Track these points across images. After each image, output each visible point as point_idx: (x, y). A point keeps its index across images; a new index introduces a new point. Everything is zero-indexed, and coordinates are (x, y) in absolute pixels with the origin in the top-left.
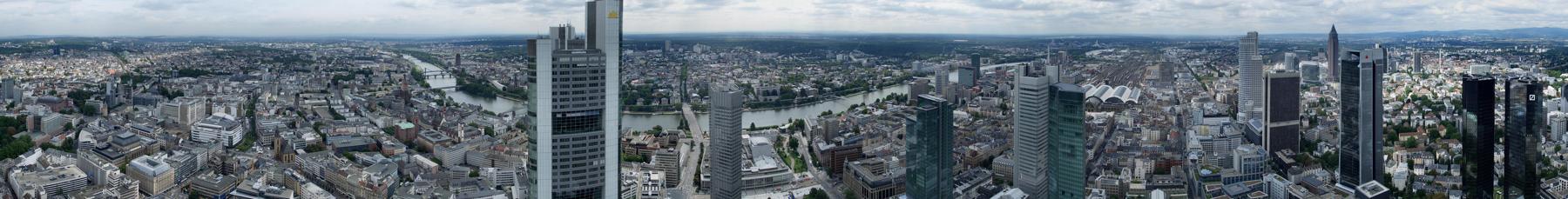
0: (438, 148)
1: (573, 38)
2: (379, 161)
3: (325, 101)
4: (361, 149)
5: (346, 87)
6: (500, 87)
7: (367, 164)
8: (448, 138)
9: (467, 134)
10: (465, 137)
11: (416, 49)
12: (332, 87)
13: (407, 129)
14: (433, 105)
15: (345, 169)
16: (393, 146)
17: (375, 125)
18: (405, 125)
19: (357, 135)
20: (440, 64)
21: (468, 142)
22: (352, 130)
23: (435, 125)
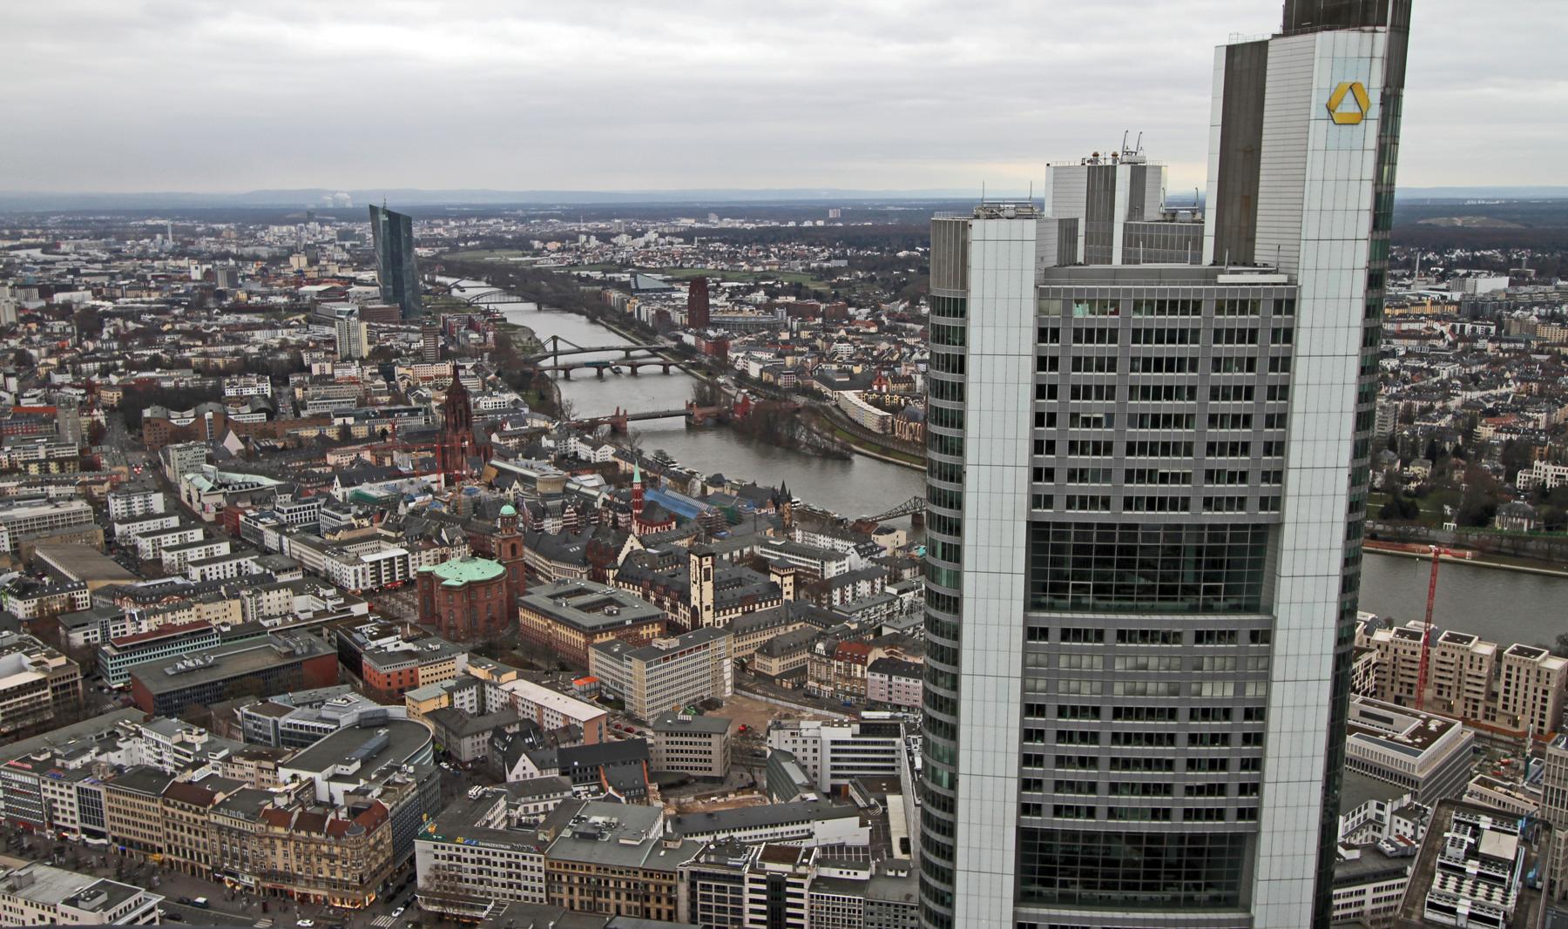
0: (605, 648)
1: (1152, 213)
2: (346, 720)
3: (79, 505)
4: (263, 685)
5: (182, 435)
6: (871, 416)
7: (297, 739)
8: (650, 610)
9: (728, 593)
10: (719, 605)
11: (514, 258)
12: (120, 433)
13: (471, 586)
14: (589, 482)
15: (198, 775)
16: (409, 654)
17: (328, 580)
18: (460, 570)
19: (249, 630)
20: (623, 322)
21: (729, 626)
22: (226, 613)
23: (597, 561)
